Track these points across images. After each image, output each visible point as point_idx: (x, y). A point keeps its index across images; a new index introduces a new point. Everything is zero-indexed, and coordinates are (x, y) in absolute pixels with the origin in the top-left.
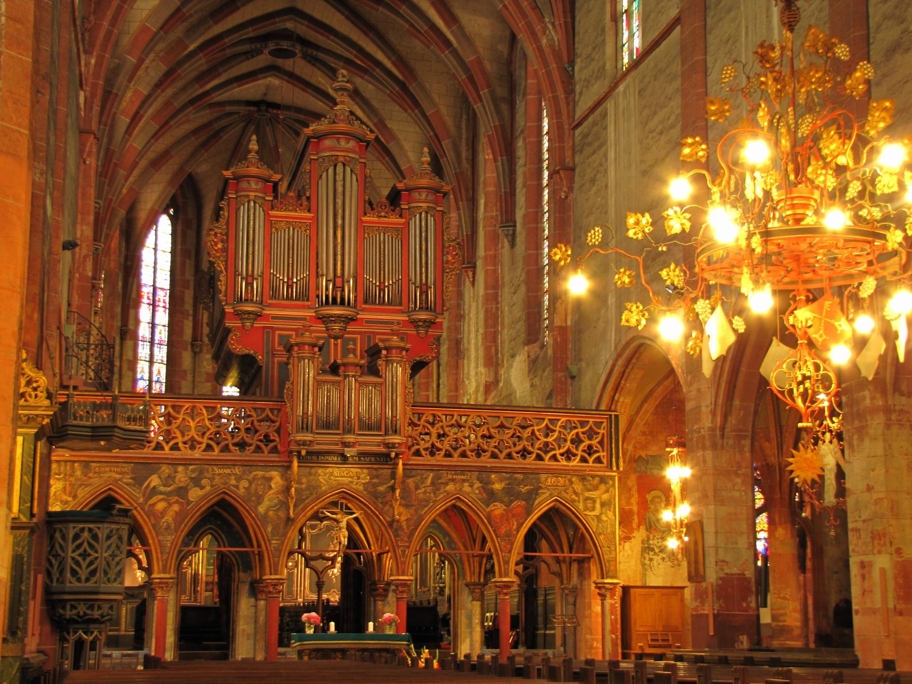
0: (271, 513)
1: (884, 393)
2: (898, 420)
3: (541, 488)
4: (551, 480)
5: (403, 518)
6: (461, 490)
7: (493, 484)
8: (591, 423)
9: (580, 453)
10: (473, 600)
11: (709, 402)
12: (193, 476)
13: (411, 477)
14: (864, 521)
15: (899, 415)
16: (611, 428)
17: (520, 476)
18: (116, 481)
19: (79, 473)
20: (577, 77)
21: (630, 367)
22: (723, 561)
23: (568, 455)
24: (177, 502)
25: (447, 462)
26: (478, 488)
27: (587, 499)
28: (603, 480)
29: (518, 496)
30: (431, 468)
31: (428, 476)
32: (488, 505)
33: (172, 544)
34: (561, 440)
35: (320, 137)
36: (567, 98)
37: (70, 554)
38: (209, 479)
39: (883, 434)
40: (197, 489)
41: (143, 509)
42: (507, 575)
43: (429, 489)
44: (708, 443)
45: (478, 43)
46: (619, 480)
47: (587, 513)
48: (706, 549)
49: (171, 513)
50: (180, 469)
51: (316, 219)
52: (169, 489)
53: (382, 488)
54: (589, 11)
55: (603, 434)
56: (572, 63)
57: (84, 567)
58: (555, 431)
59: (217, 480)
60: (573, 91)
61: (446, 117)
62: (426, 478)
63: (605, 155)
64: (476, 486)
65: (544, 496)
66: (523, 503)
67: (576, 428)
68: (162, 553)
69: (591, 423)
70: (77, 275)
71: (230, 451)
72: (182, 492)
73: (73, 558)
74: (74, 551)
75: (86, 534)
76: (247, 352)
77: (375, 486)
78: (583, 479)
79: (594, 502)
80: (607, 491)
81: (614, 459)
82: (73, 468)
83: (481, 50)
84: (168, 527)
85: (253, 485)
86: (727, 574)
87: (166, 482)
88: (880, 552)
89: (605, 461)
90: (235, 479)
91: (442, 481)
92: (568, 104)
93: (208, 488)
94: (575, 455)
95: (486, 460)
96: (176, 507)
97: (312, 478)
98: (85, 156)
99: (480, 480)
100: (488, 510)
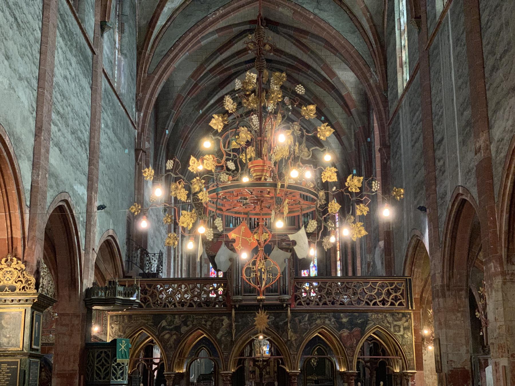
0: (223, 338)
1: (501, 265)
2: (510, 279)
3: (369, 320)
4: (374, 316)
5: (293, 339)
6: (324, 322)
7: (342, 319)
8: (396, 284)
9: (390, 300)
10: (344, 382)
11: (439, 271)
14: (495, 338)
15: (511, 276)
16: (407, 286)
18: (144, 325)
19: (126, 321)
20: (389, 98)
21: (417, 252)
22: (451, 361)
23: (383, 302)
26: (333, 322)
27: (396, 325)
28: (404, 315)
29: (356, 325)
30: (307, 311)
31: (306, 315)
32: (339, 331)
34: (379, 294)
36: (385, 110)
37: (95, 365)
39: (502, 287)
40: (185, 327)
41: (158, 338)
42: (352, 369)
43: (306, 323)
44: (440, 294)
45: (347, 85)
46: (414, 314)
47: (396, 333)
48: (442, 354)
52: (171, 327)
53: (281, 323)
54: (392, 63)
56: (386, 91)
57: (102, 371)
59: (195, 323)
60: (388, 106)
61: (343, 125)
63: (400, 139)
64: (332, 320)
65: (371, 325)
66: (359, 329)
69: (396, 284)
71: (201, 306)
72: (177, 328)
73: (97, 367)
74: (97, 363)
75: (103, 355)
78: (392, 315)
79: (400, 327)
80: (407, 321)
81: (410, 303)
82: (123, 318)
83: (350, 89)
84: (171, 347)
85: (213, 324)
86: (455, 368)
87: (170, 323)
88: (502, 357)
89: (405, 304)
92: (385, 113)
93: (191, 326)
94: (388, 302)
96: (175, 337)
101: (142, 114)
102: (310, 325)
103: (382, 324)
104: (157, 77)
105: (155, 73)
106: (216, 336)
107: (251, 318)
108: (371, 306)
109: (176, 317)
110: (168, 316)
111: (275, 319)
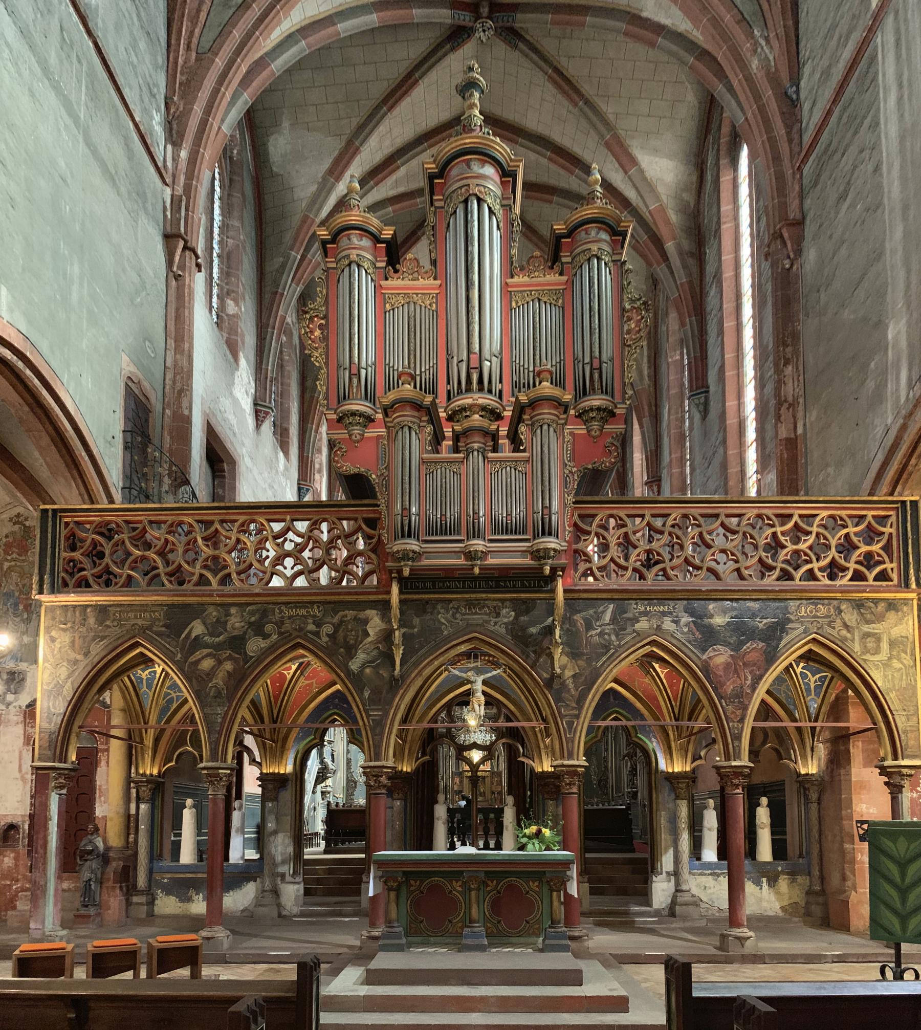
0: (368, 671)
3: (789, 621)
4: (805, 610)
6: (659, 628)
7: (711, 616)
9: (852, 566)
12: (253, 619)
13: (579, 612)
19: (92, 621)
23: (834, 570)
24: (229, 658)
25: (637, 584)
26: (687, 625)
28: (892, 605)
32: (704, 650)
33: (224, 718)
34: (820, 548)
38: (275, 623)
41: (181, 670)
42: (738, 757)
49: (221, 675)
52: (217, 639)
53: (533, 630)
55: (891, 534)
58: (810, 533)
59: (287, 626)
62: (603, 612)
66: (761, 644)
67: (845, 527)
68: (209, 733)
69: (870, 518)
72: (237, 643)
78: (859, 605)
79: (878, 640)
84: (218, 695)
87: (217, 627)
89: (895, 576)
90: (314, 623)
91: (629, 615)
93: (275, 637)
94: (844, 569)
95: (701, 581)
96: (228, 666)
97: (428, 617)
99: (691, 612)
100: (704, 657)
102: (617, 636)
103: (830, 630)
106: (346, 666)
107: (449, 616)
108: (797, 582)
109: (233, 611)
110: (211, 609)
111: (516, 618)
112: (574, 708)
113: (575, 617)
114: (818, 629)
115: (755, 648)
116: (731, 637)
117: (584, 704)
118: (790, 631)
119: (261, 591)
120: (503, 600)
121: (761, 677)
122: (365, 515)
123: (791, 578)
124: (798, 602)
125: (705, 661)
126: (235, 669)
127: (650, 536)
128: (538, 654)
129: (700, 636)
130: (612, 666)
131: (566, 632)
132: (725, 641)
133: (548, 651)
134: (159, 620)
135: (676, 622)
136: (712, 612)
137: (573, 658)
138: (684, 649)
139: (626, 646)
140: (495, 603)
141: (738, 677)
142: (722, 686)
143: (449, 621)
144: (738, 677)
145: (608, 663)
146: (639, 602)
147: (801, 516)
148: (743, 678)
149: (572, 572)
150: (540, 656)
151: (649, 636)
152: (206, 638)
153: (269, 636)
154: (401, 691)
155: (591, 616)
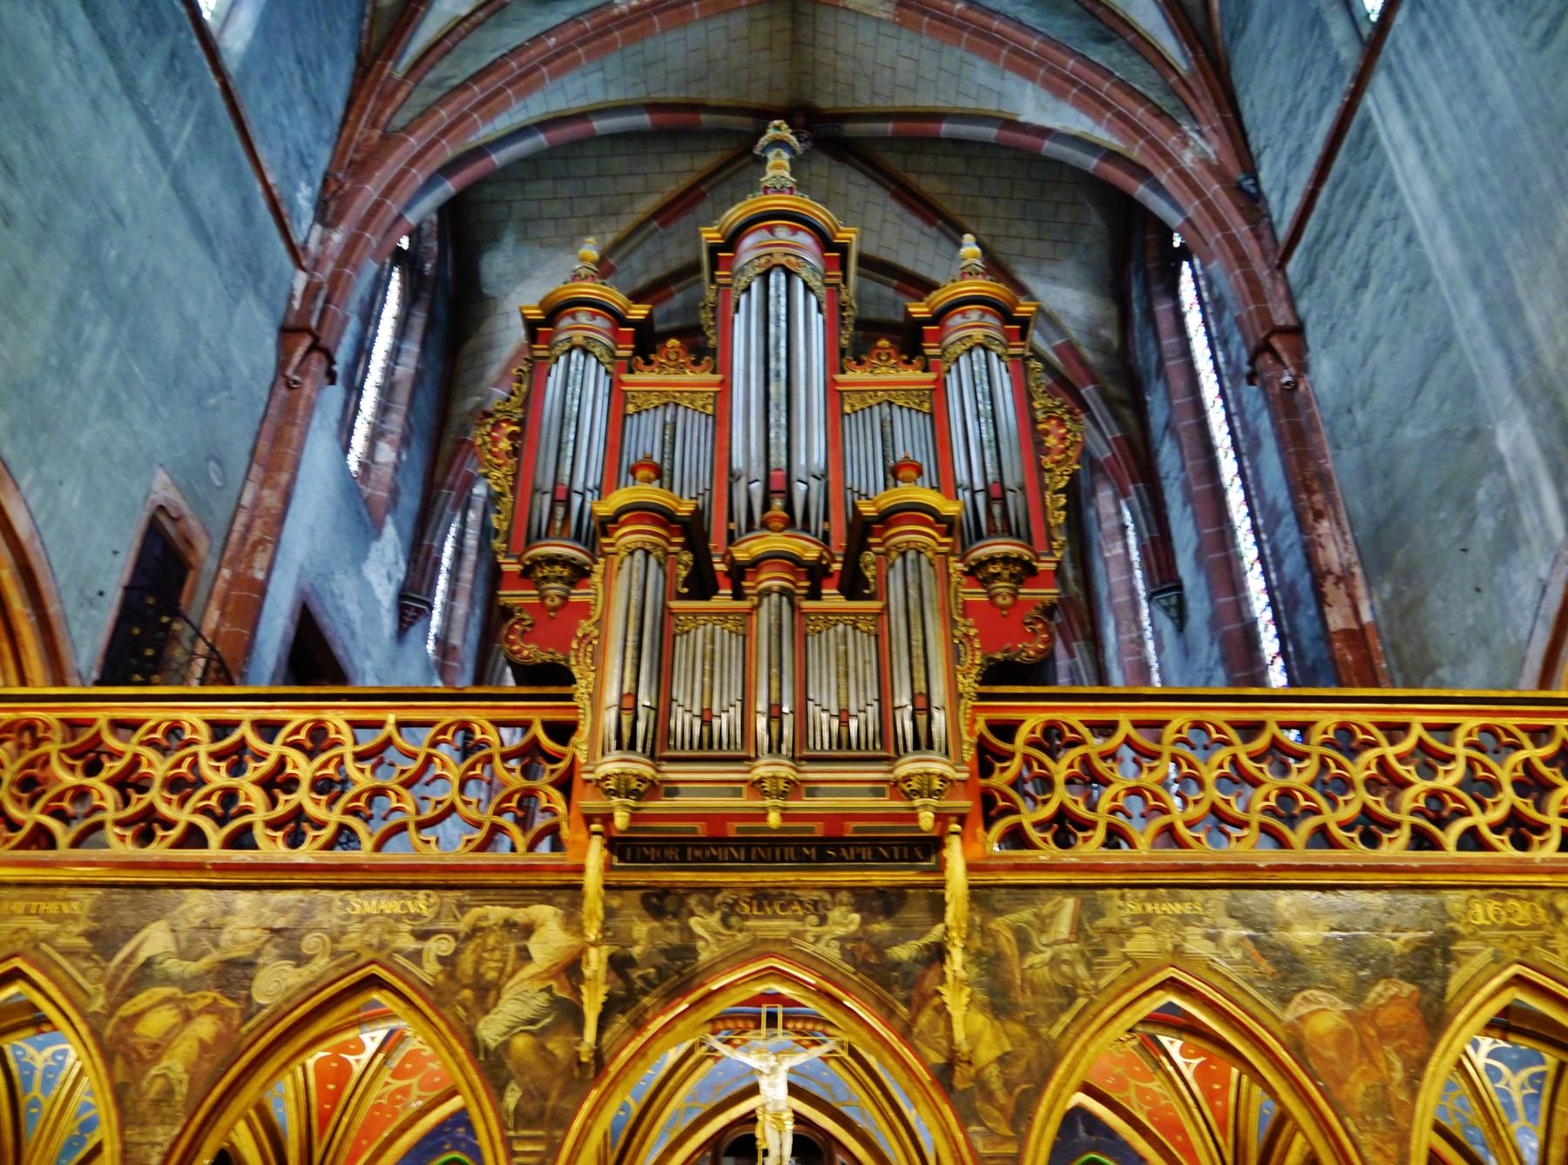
0: (521, 1043)
3: (1454, 935)
4: (1483, 910)
5: (987, 1053)
6: (1178, 950)
7: (1287, 926)
12: (280, 923)
13: (999, 913)
17: (1378, 899)
18: (35, 942)
24: (211, 1009)
26: (1237, 943)
32: (1284, 1000)
34: (1481, 787)
35: (732, 241)
40: (287, 966)
41: (96, 1033)
43: (1068, 951)
50: (243, 900)
51: (726, 386)
52: (193, 967)
62: (1052, 915)
66: (1408, 989)
67: (1518, 747)
70: (226, 573)
76: (547, 657)
77: (879, 948)
91: (1110, 921)
92: (1258, 237)
93: (321, 964)
96: (205, 1027)
98: (289, 372)
100: (1288, 1016)
101: (337, 237)
102: (1089, 965)
104: (414, 142)
105: (408, 129)
107: (714, 920)
111: (864, 922)
112: (1006, 1139)
113: (993, 925)
114: (1523, 952)
115: (1394, 997)
116: (1337, 971)
117: (1030, 1127)
118: (1463, 958)
119: (311, 861)
120: (833, 890)
121: (1422, 1063)
122: (550, 716)
123: (1436, 845)
124: (1465, 894)
125: (1291, 1026)
126: (219, 1037)
127: (1135, 761)
128: (916, 1004)
129: (1271, 969)
130: (1085, 1037)
131: (975, 956)
132: (1327, 981)
133: (936, 1001)
134: (75, 918)
135: (1212, 938)
136: (1286, 915)
137: (996, 1017)
138: (1239, 997)
139: (1113, 991)
140: (815, 895)
141: (1372, 1062)
142: (1340, 1082)
143: (715, 933)
144: (1372, 1062)
145: (1075, 1029)
146: (1128, 893)
147: (1428, 727)
148: (1383, 1065)
149: (980, 831)
150: (919, 1010)
151: (1159, 969)
152: (168, 963)
153: (309, 959)
154: (594, 1094)
155: (1028, 923)
